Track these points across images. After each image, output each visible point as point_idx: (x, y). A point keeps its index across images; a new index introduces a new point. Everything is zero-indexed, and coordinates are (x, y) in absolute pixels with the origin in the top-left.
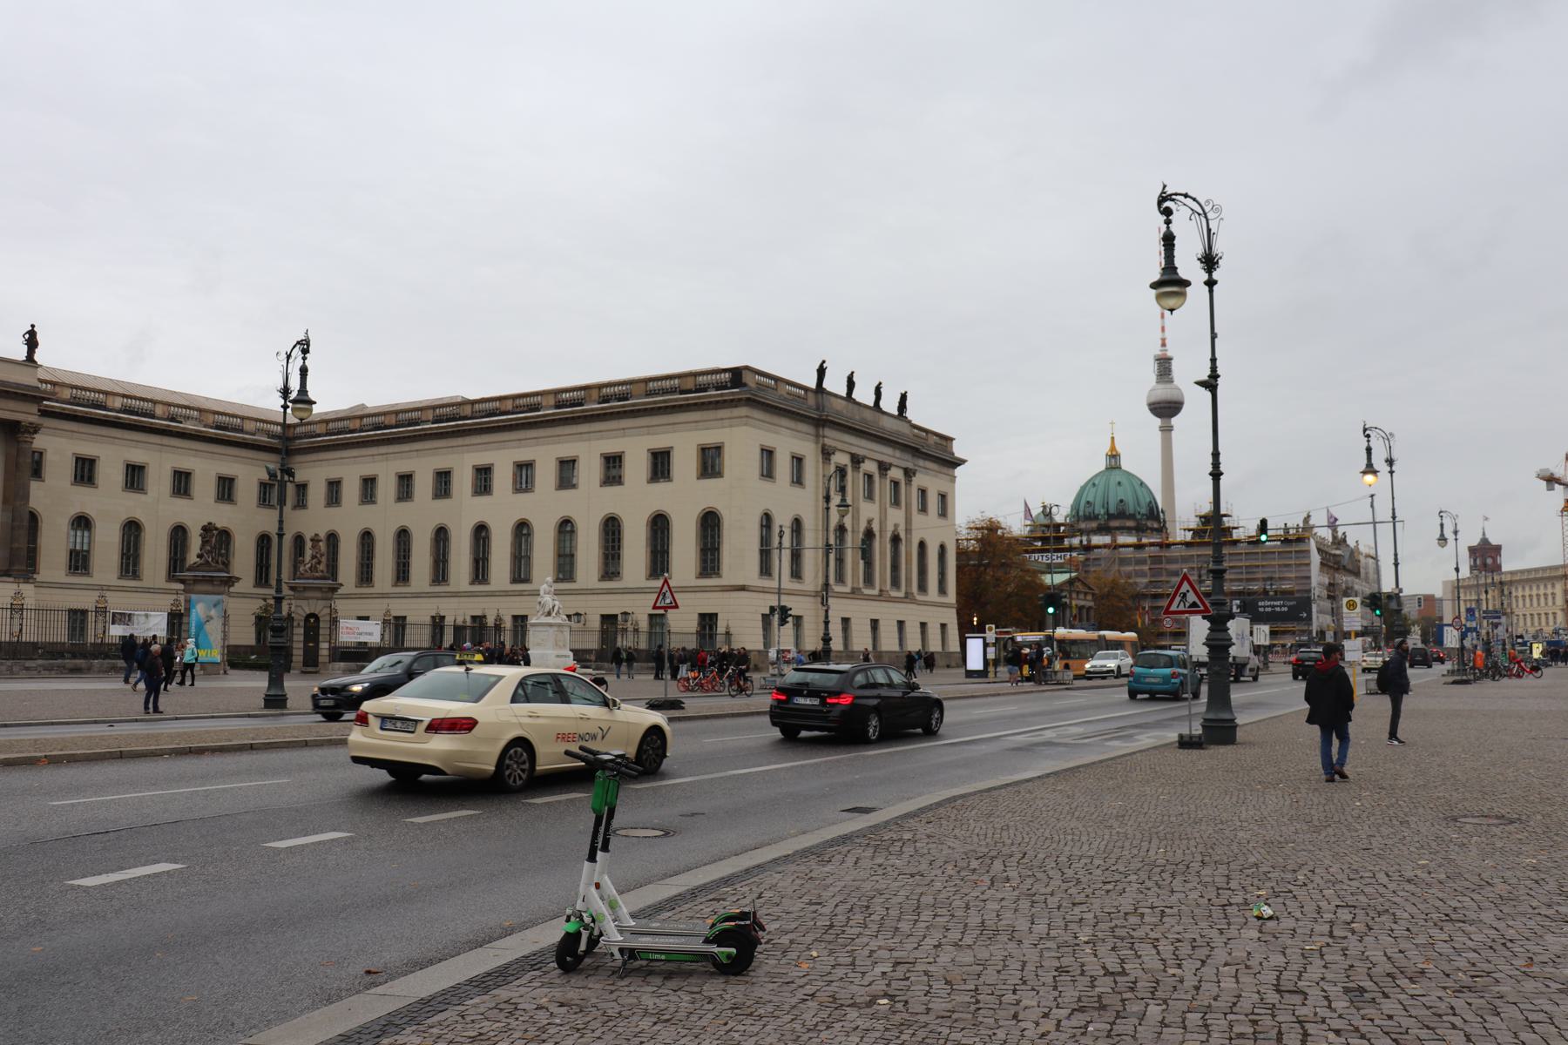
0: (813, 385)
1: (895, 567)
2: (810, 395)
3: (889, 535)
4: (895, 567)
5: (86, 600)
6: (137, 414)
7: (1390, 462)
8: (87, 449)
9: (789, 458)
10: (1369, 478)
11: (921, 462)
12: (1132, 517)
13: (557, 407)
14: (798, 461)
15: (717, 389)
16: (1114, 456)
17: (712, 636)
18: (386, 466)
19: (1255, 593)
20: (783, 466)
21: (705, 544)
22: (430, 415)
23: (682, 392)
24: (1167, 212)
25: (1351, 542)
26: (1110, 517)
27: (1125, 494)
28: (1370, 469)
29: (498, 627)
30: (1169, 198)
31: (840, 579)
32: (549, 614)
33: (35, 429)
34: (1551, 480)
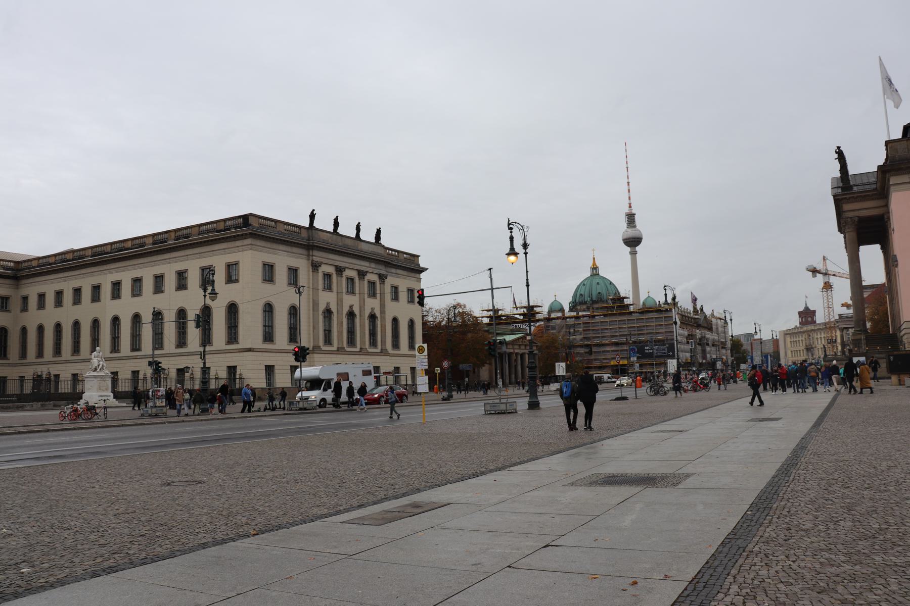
1: (373, 334)
2: (304, 232)
3: (367, 314)
4: (373, 334)
7: (525, 246)
9: (286, 269)
10: (512, 258)
13: (154, 244)
14: (293, 272)
15: (236, 228)
16: (595, 268)
17: (235, 380)
18: (67, 284)
19: (643, 342)
20: (281, 275)
21: (231, 324)
22: (89, 252)
23: (217, 231)
25: (708, 312)
26: (594, 302)
27: (601, 289)
28: (512, 252)
29: (49, 380)
32: (95, 370)
34: (814, 271)
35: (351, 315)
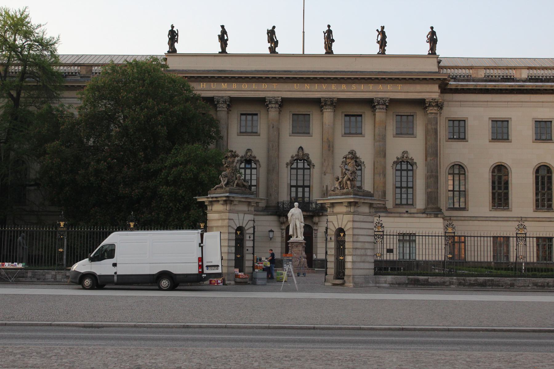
5: (508, 229)
6: (541, 81)
8: (500, 113)
33: (440, 106)
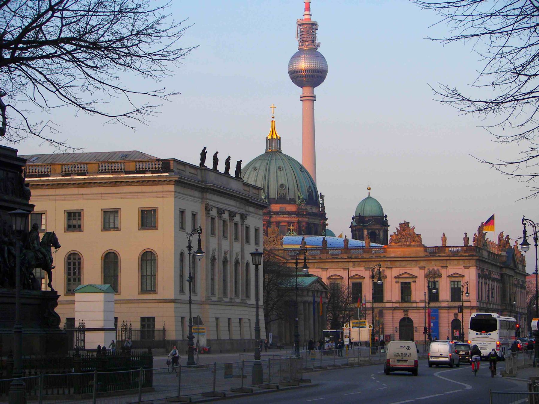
0: (198, 164)
11: (251, 209)
12: (292, 201)
24: (525, 224)
30: (526, 220)
31: (213, 293)
35: (225, 262)
